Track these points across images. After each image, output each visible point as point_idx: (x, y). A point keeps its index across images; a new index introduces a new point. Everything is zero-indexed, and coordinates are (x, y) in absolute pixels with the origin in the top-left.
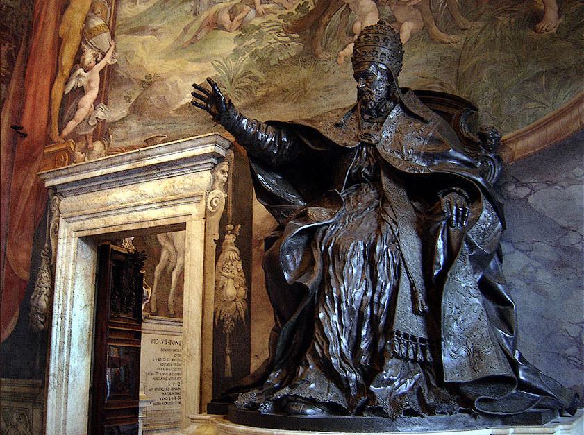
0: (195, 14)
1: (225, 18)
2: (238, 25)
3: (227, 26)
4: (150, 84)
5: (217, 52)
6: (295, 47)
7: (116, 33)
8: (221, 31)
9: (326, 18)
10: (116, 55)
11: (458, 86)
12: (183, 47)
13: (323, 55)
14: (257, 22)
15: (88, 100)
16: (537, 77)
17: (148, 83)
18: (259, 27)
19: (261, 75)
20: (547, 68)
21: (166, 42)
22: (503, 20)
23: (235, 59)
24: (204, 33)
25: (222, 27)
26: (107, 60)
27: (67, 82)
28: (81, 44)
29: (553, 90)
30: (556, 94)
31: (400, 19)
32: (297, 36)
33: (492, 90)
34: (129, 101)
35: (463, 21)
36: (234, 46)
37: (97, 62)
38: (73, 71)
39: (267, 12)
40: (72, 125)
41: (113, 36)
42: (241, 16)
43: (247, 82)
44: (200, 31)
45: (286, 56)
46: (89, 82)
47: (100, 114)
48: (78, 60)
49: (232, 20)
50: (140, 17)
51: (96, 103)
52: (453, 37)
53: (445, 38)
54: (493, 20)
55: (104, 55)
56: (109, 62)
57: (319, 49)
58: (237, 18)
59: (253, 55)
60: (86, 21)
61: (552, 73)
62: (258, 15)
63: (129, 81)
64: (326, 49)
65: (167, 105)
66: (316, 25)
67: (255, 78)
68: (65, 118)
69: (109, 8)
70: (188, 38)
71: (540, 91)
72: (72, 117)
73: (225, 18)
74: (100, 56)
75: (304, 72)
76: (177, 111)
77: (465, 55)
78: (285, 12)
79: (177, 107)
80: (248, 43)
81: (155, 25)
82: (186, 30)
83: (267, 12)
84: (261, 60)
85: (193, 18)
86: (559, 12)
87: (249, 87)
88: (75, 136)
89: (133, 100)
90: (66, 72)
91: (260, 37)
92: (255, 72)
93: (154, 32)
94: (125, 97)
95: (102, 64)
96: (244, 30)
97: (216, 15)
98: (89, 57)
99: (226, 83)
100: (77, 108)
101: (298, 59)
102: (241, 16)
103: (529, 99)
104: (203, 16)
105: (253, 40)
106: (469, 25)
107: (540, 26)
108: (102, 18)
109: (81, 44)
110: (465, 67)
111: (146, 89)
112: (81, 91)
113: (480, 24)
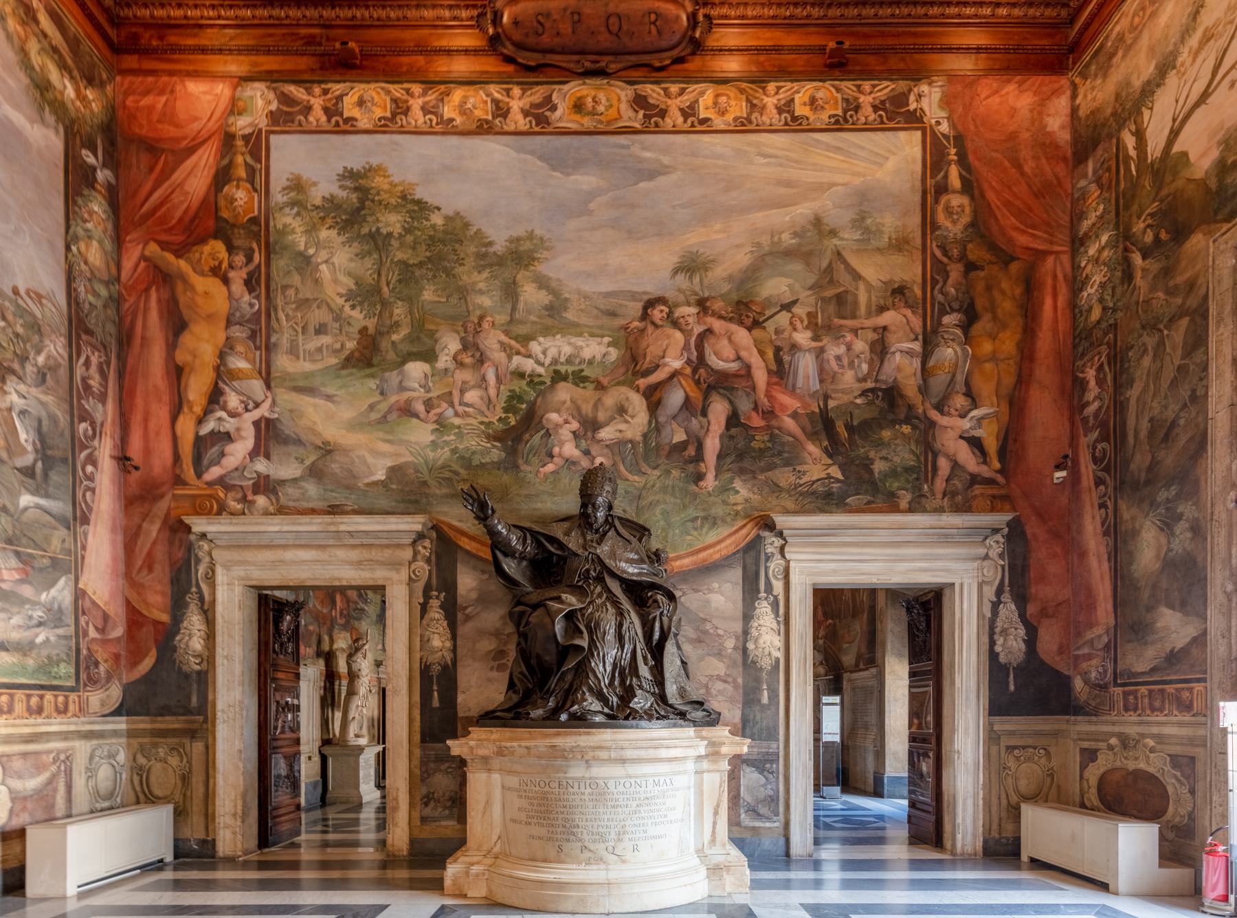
0: (382, 393)
1: (420, 408)
2: (435, 418)
3: (422, 416)
4: (329, 452)
5: (413, 439)
6: (496, 454)
7: (273, 384)
8: (415, 420)
9: (527, 436)
10: (277, 409)
11: (637, 514)
12: (369, 424)
13: (524, 467)
14: (457, 421)
15: (238, 451)
16: (695, 519)
17: (327, 450)
18: (459, 427)
19: (462, 471)
20: (702, 514)
21: (347, 413)
22: (675, 473)
23: (433, 451)
24: (394, 415)
25: (417, 416)
26: (264, 411)
27: (200, 422)
28: (217, 383)
29: (705, 530)
30: (707, 533)
31: (593, 453)
32: (498, 444)
33: (662, 523)
34: (302, 461)
35: (645, 468)
36: (432, 438)
37: (247, 410)
38: (207, 412)
39: (467, 415)
40: (214, 473)
41: (268, 387)
42: (438, 410)
43: (447, 474)
44: (389, 411)
45: (488, 460)
46: (238, 430)
47: (261, 466)
48: (215, 398)
49: (428, 412)
50: (307, 375)
51: (254, 454)
52: (636, 478)
53: (630, 477)
54: (668, 472)
55: (257, 405)
56: (267, 414)
57: (520, 462)
58: (433, 412)
59: (454, 451)
60: (222, 355)
61: (705, 518)
62: (457, 414)
63: (299, 442)
64: (527, 462)
65: (355, 477)
66: (518, 439)
67: (456, 473)
68: (205, 462)
69: (258, 353)
70: (374, 416)
71: (696, 529)
72: (216, 462)
73: (420, 408)
74: (251, 406)
75: (506, 478)
76: (368, 485)
77: (644, 493)
78: (486, 420)
79: (367, 481)
80: (446, 438)
81: (330, 390)
82: (372, 407)
83: (467, 415)
84: (462, 458)
85: (379, 398)
86: (716, 476)
87: (449, 479)
88: (221, 481)
89: (308, 462)
90: (198, 409)
91: (460, 435)
92: (456, 467)
93: (329, 398)
94: (297, 459)
95: (256, 414)
96: (442, 426)
97: (409, 402)
98: (233, 401)
99: (425, 471)
100: (223, 454)
101: (497, 465)
102: (438, 410)
103: (688, 534)
104: (393, 399)
105: (452, 437)
106: (649, 471)
107: (701, 483)
108: (247, 360)
109: (217, 383)
110: (644, 503)
111: (324, 456)
112: (227, 437)
113: (657, 473)
